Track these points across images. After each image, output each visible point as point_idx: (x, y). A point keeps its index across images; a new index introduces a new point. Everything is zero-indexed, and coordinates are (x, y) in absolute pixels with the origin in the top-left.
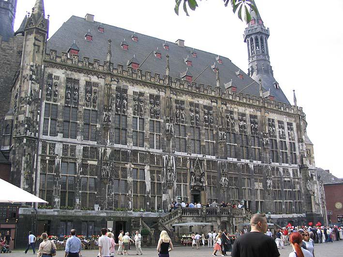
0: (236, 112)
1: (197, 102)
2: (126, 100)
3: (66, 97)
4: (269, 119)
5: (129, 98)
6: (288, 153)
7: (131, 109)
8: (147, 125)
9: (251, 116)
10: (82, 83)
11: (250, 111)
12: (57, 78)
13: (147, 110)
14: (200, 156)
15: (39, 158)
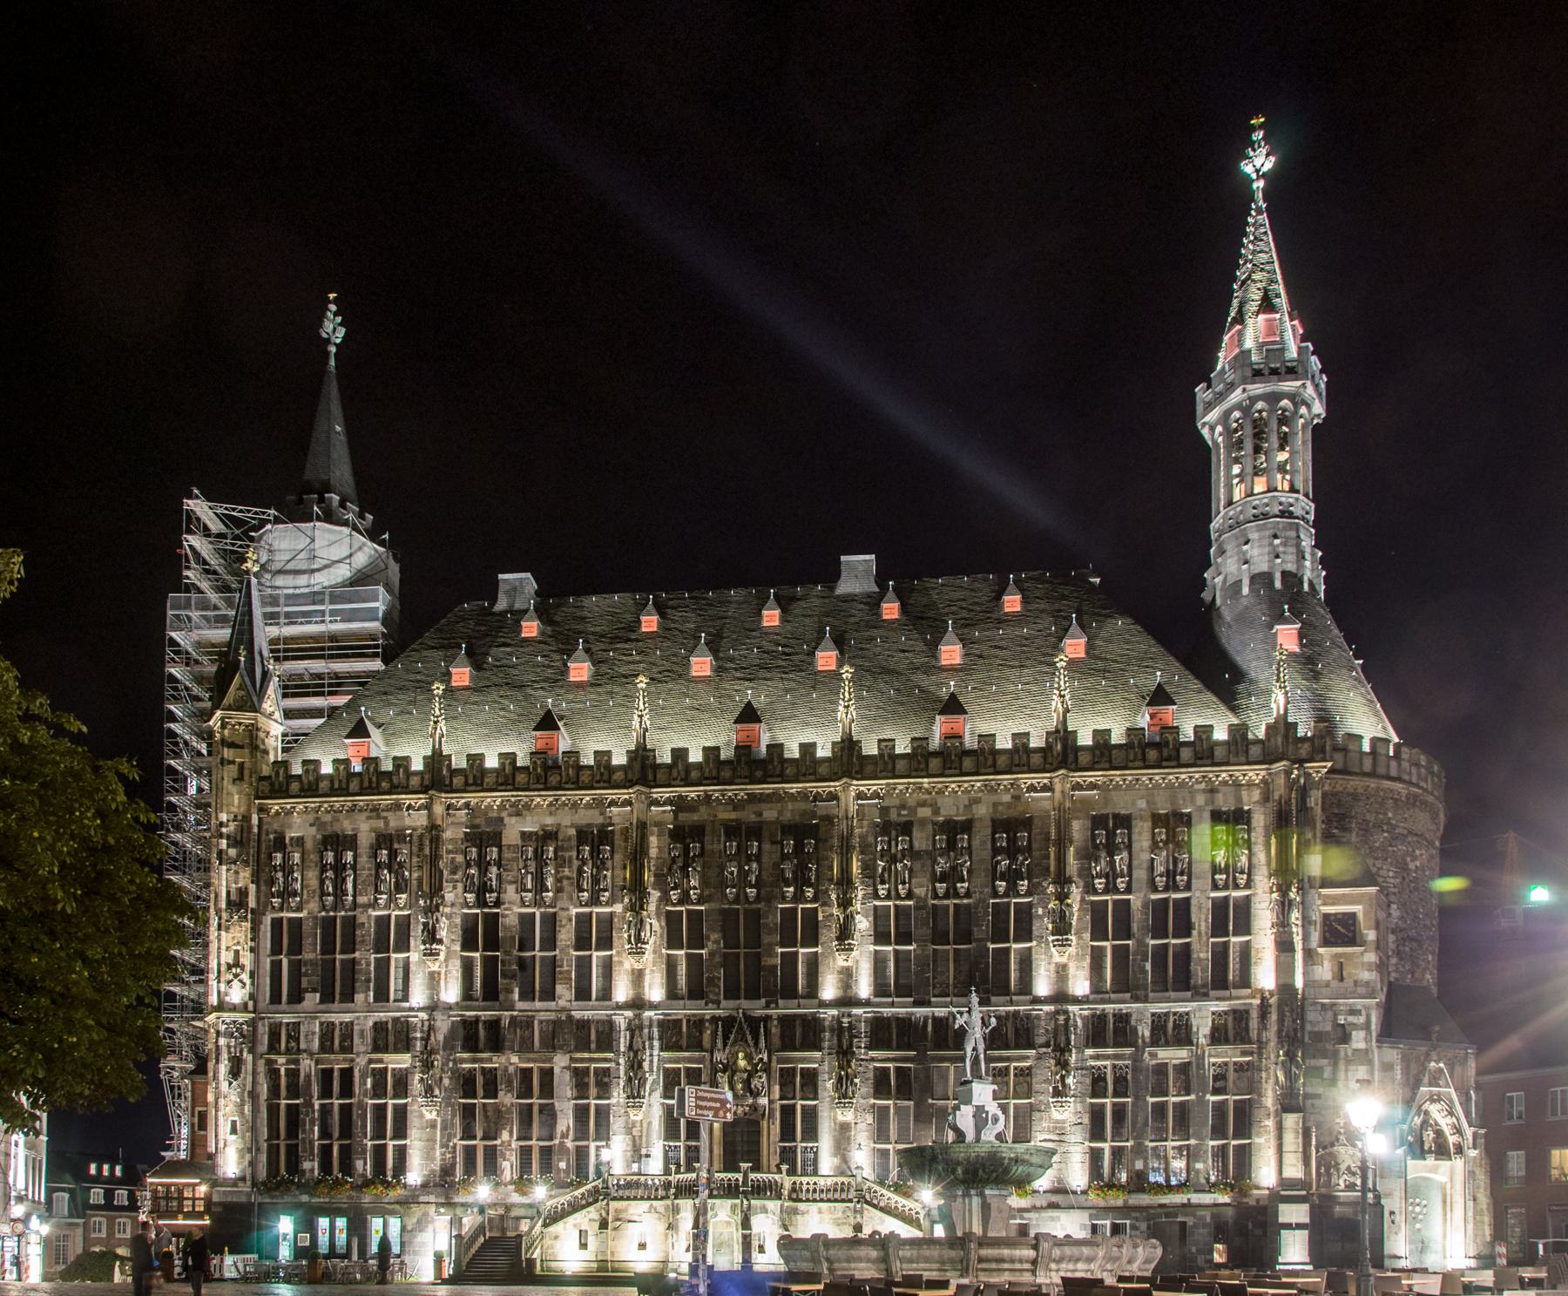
0: (923, 822)
1: (753, 818)
2: (499, 865)
3: (323, 894)
4: (1098, 822)
5: (507, 855)
6: (1195, 947)
7: (511, 889)
8: (563, 930)
9: (998, 825)
10: (365, 840)
11: (995, 805)
12: (300, 841)
13: (565, 882)
14: (757, 1009)
15: (261, 1062)
